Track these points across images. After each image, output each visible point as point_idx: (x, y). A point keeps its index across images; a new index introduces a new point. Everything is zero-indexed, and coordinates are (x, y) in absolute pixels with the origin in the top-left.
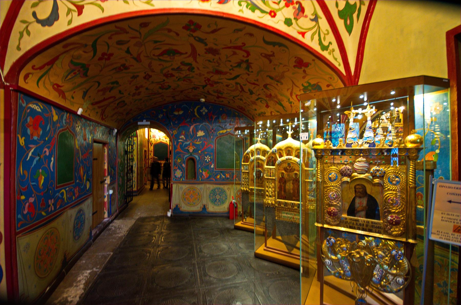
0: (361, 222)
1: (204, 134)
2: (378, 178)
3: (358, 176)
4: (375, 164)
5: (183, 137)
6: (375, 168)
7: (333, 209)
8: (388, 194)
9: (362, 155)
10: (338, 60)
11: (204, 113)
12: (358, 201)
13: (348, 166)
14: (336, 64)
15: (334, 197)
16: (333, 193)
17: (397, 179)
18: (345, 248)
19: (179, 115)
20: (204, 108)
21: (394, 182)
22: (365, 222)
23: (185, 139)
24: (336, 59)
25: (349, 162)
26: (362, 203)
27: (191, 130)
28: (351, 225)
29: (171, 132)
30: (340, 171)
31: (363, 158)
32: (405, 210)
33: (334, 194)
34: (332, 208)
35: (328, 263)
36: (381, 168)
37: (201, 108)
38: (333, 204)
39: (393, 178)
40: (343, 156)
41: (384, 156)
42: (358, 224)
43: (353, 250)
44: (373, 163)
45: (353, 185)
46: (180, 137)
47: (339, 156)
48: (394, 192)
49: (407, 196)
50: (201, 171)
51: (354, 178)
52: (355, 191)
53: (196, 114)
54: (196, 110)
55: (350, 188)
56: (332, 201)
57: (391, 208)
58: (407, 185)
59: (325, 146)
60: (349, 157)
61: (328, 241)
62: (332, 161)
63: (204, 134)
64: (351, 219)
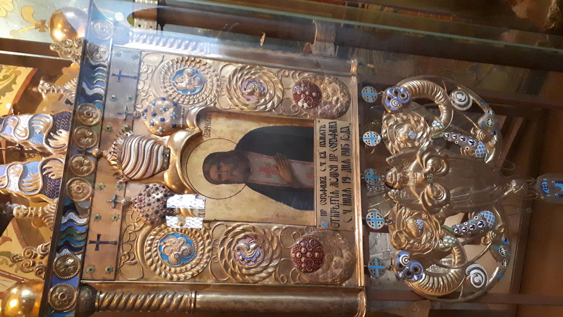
0: (327, 174)
15: (253, 246)
22: (323, 161)
28: (341, 199)
30: (152, 223)
33: (241, 244)
40: (95, 212)
52: (227, 182)
64: (323, 199)
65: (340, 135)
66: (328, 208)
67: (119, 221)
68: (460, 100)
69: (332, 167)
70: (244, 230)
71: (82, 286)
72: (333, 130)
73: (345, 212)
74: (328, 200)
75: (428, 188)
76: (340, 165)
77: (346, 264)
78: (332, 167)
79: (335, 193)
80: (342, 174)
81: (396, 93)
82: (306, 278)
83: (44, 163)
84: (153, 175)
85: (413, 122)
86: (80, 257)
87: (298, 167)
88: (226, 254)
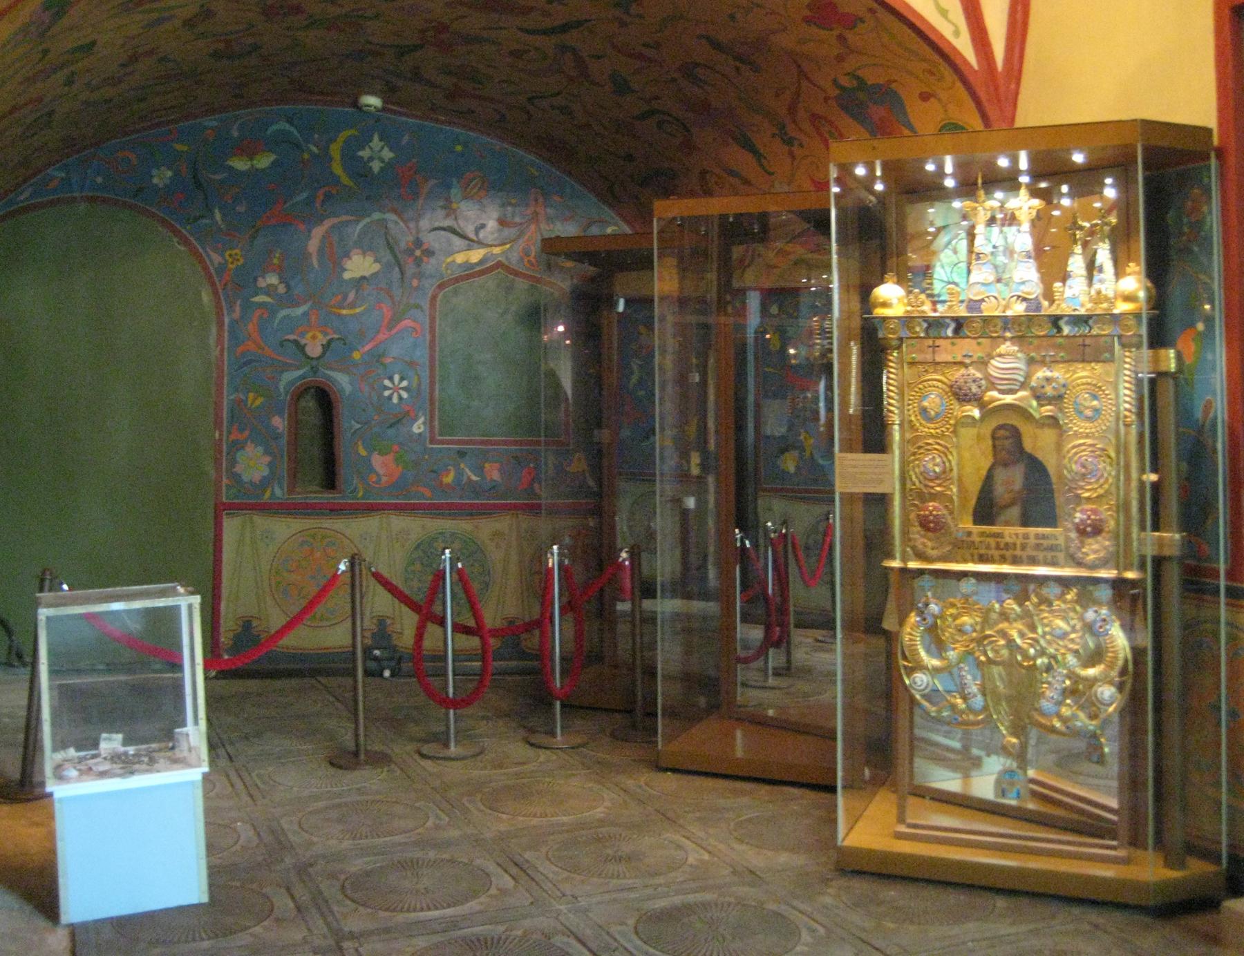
0: (1008, 539)
1: (376, 267)
2: (1049, 404)
3: (1000, 400)
4: (1043, 363)
5: (272, 279)
6: (1042, 373)
7: (935, 509)
8: (1074, 447)
9: (1008, 334)
10: (951, 16)
11: (376, 166)
12: (1001, 475)
13: (972, 370)
14: (946, 30)
15: (937, 469)
16: (934, 458)
17: (1095, 403)
18: (968, 628)
19: (254, 173)
20: (376, 142)
21: (1088, 413)
22: (1020, 537)
23: (282, 289)
24: (944, 13)
25: (975, 358)
26: (1012, 480)
27: (313, 245)
28: (983, 551)
29: (216, 258)
30: (951, 387)
31: (1013, 344)
32: (1113, 489)
33: (938, 460)
34: (931, 504)
35: (919, 683)
36: (1055, 374)
37: (364, 141)
38: (932, 491)
39: (1085, 399)
40: (957, 341)
41: (1062, 337)
42: (1002, 546)
43: (990, 629)
44: (1038, 358)
45: (987, 429)
46: (262, 283)
47: (949, 341)
48: (1089, 441)
49: (1118, 453)
50: (363, 452)
51: (991, 406)
52: (994, 446)
53: (337, 169)
54: (335, 150)
55: (979, 438)
56: (931, 484)
57: (1082, 488)
58: (1118, 419)
59: (909, 308)
60: (974, 342)
61: (921, 613)
62: (929, 357)
63: (376, 267)
64: (982, 534)
65: (1049, 555)
66: (977, 539)
67: (953, 360)
68: (1102, 693)
69: (1015, 544)
70: (949, 461)
71: (901, 339)
72: (1051, 548)
73: (972, 555)
74: (982, 539)
75: (1002, 642)
76: (1018, 552)
77: (924, 553)
78: (1015, 544)
79: (988, 547)
80: (1008, 554)
81: (1104, 620)
82: (912, 516)
83: (995, 297)
84: (993, 383)
85: (1073, 636)
86: (922, 335)
87: (1015, 512)
88: (929, 447)
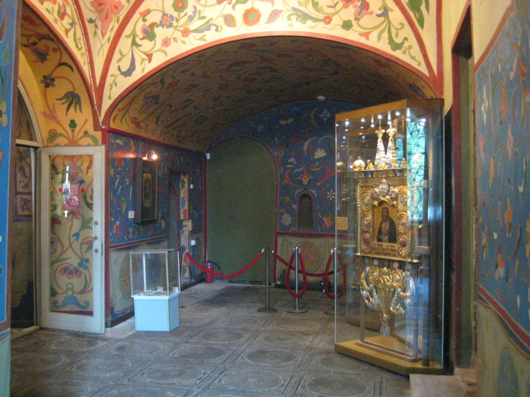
1: (325, 154)
5: (293, 160)
10: (416, 59)
11: (325, 119)
14: (414, 64)
19: (287, 125)
20: (325, 111)
23: (295, 163)
24: (413, 58)
27: (305, 148)
29: (276, 154)
37: (322, 110)
46: (289, 161)
50: (321, 217)
53: (313, 121)
54: (312, 115)
63: (325, 154)
